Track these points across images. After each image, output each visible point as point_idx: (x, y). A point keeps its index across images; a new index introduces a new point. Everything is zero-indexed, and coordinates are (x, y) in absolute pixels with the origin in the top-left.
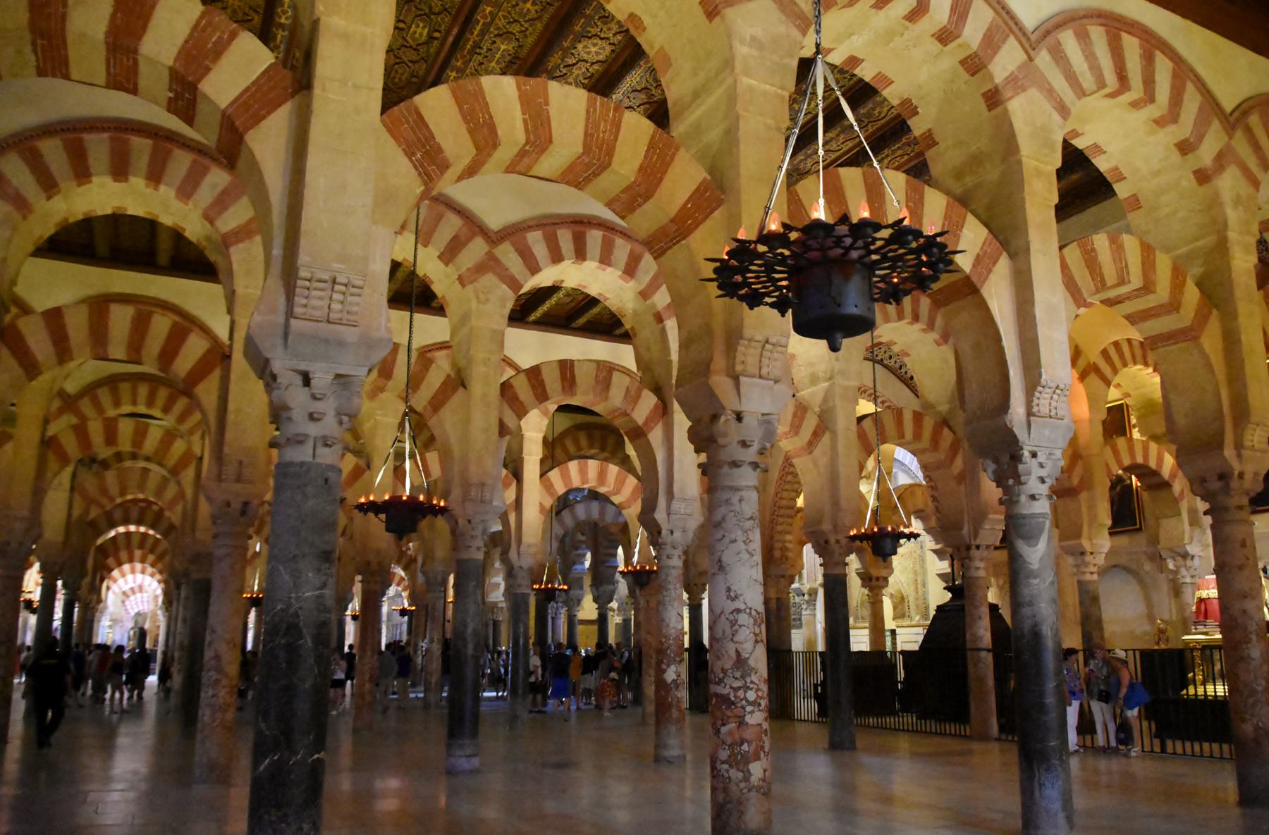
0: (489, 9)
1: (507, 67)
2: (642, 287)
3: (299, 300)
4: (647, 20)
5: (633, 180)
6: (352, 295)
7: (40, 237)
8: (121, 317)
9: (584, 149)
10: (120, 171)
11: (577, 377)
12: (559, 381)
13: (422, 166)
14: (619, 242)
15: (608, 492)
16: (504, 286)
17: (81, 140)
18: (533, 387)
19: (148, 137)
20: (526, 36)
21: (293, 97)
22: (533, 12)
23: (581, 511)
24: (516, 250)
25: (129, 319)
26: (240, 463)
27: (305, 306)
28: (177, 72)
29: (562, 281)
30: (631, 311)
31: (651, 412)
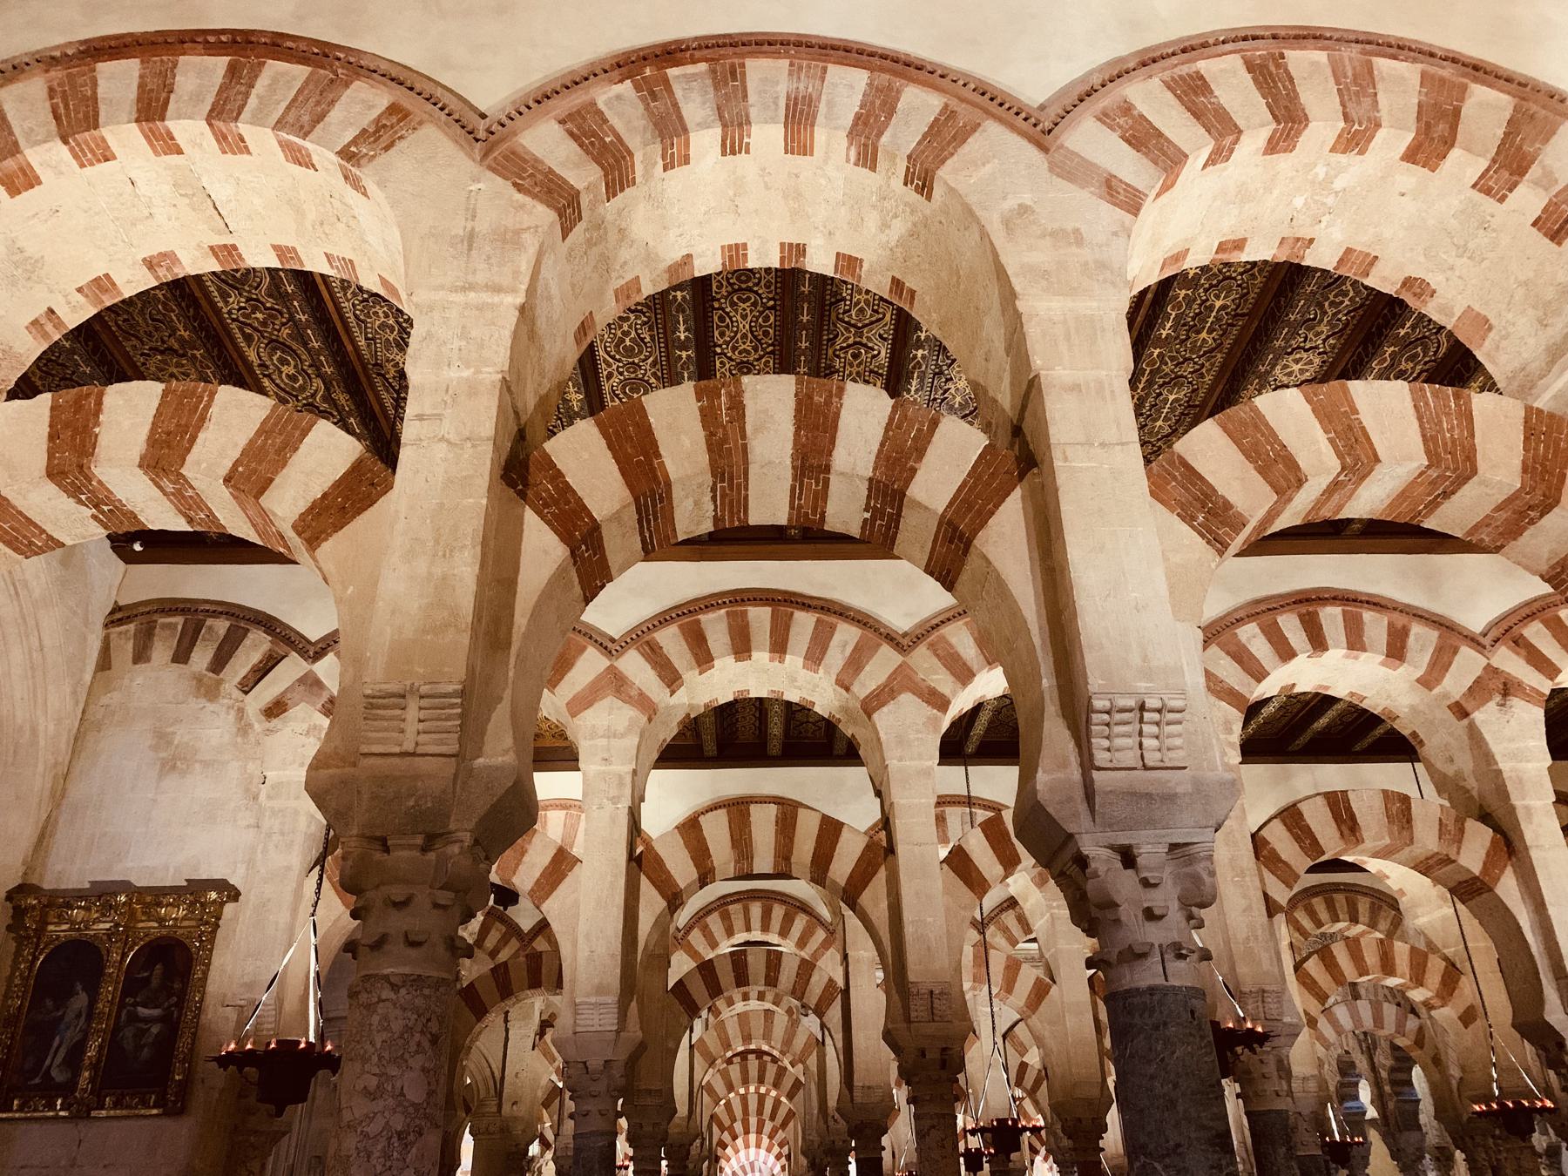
0: (1157, 352)
1: (1177, 421)
2: (1420, 673)
3: (1098, 743)
4: (1434, 280)
5: (1519, 486)
6: (1168, 724)
7: (664, 740)
8: (763, 822)
9: (1429, 459)
10: (742, 647)
11: (1358, 816)
12: (1334, 824)
13: (1210, 531)
14: (1368, 616)
17: (698, 622)
18: (1297, 839)
20: (1202, 376)
21: (1021, 477)
22: (1210, 341)
24: (1228, 653)
25: (773, 819)
27: (1109, 750)
28: (879, 482)
31: (1488, 855)
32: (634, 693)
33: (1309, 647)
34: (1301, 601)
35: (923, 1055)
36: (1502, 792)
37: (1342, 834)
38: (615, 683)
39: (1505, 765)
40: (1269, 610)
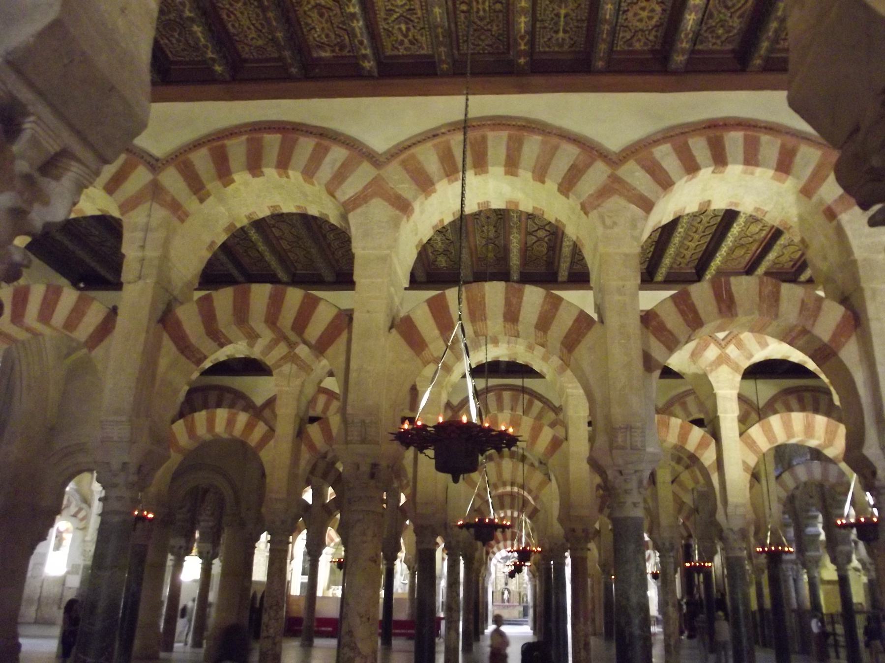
12: (714, 303)
14: (765, 138)
15: (820, 445)
16: (633, 207)
17: (223, 147)
18: (683, 313)
19: (277, 132)
23: (801, 472)
26: (363, 421)
29: (709, 202)
30: (796, 219)
31: (838, 326)
32: (168, 199)
33: (711, 162)
34: (709, 127)
35: (358, 468)
36: (855, 279)
37: (720, 311)
38: (155, 191)
39: (858, 254)
40: (682, 133)
